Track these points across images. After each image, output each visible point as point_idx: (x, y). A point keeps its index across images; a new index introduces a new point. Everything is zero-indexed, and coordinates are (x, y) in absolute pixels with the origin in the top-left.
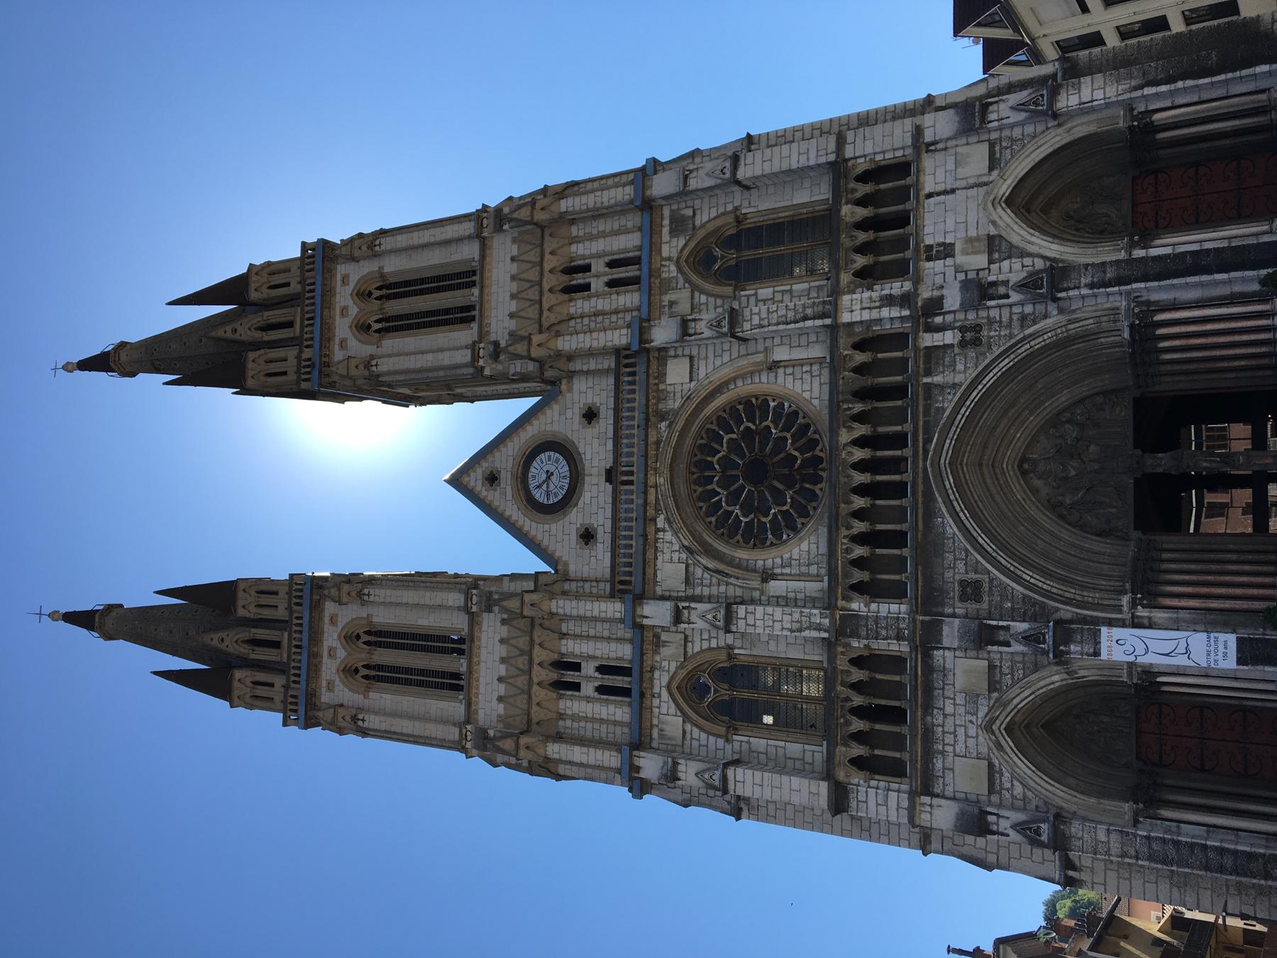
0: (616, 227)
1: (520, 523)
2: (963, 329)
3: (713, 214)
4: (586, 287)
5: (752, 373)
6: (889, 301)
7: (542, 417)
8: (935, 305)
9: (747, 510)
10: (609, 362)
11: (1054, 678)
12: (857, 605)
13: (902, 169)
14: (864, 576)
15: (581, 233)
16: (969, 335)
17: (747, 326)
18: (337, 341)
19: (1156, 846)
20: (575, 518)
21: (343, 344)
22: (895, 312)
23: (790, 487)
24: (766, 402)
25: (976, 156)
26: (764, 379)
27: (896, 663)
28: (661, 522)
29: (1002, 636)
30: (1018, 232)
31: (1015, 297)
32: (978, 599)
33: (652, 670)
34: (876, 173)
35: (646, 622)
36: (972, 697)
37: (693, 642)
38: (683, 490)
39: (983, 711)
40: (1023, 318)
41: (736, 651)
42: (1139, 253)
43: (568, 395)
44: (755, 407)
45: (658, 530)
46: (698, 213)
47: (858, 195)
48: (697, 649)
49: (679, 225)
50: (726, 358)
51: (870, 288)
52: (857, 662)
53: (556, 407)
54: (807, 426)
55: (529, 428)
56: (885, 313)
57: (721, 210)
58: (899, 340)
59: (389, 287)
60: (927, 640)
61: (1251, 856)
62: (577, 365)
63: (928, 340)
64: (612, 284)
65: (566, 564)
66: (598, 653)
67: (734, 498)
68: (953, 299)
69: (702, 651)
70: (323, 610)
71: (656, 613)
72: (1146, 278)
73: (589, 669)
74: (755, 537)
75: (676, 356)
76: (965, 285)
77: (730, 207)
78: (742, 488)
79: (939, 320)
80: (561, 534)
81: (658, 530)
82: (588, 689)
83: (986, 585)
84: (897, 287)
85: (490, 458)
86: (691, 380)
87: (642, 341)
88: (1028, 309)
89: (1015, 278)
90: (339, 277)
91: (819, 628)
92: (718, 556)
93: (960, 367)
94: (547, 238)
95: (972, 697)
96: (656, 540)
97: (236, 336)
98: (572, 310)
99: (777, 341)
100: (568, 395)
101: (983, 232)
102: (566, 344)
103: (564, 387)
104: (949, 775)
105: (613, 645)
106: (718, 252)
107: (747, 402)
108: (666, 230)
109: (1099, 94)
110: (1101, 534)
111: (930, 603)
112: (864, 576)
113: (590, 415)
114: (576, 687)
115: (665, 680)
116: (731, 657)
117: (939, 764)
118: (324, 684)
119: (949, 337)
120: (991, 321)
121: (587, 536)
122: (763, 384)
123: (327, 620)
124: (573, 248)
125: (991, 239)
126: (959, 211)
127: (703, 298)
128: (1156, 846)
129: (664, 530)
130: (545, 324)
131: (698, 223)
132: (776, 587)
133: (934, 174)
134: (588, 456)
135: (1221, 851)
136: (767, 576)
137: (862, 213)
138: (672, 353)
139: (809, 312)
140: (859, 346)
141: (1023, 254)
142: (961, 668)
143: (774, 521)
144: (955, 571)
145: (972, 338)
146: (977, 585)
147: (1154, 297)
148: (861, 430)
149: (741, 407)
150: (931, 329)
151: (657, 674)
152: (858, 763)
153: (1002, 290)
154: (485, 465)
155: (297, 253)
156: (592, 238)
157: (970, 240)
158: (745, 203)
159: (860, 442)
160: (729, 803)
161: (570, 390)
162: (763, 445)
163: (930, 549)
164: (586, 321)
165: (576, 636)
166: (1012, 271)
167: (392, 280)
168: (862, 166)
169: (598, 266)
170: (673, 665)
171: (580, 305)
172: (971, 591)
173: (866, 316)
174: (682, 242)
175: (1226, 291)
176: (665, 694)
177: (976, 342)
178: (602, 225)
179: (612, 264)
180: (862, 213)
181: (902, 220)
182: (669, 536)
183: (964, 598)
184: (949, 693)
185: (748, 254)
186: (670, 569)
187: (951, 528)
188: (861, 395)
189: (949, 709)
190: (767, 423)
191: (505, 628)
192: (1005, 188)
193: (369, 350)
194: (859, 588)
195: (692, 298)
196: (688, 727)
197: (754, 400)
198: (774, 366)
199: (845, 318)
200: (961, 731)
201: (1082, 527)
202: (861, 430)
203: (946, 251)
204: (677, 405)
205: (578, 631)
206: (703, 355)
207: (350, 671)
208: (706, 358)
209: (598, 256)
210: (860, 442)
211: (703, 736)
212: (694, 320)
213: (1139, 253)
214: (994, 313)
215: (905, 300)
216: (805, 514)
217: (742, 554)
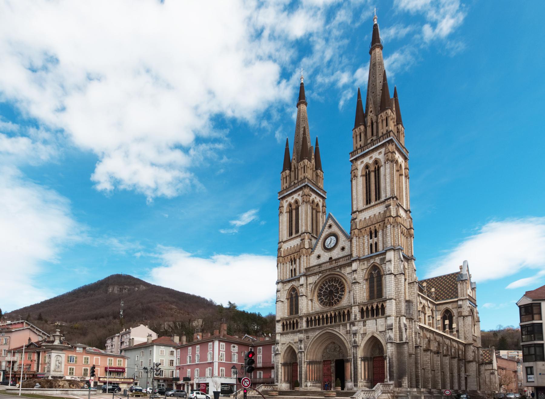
6: (356, 316)
8: (354, 325)
12: (305, 319)
14: (309, 319)
22: (353, 318)
23: (329, 300)
30: (366, 338)
31: (353, 340)
36: (293, 340)
38: (327, 277)
39: (292, 342)
44: (343, 290)
52: (297, 321)
56: (353, 316)
60: (300, 332)
63: (348, 325)
68: (354, 328)
74: (319, 295)
76: (356, 330)
89: (357, 339)
92: (315, 289)
95: (293, 340)
107: (344, 287)
111: (306, 331)
112: (309, 319)
122: (347, 290)
126: (373, 327)
132: (310, 302)
136: (311, 300)
137: (375, 307)
140: (348, 311)
145: (348, 332)
148: (333, 315)
152: (283, 323)
157: (366, 330)
159: (331, 315)
162: (335, 293)
163: (313, 330)
166: (358, 338)
169: (375, 240)
172: (308, 338)
173: (353, 312)
177: (347, 333)
180: (375, 307)
182: (318, 277)
185: (375, 280)
186: (311, 280)
187: (317, 333)
188: (339, 313)
194: (308, 319)
202: (333, 315)
203: (364, 325)
204: (343, 272)
210: (331, 315)
215: (355, 319)
217: (316, 294)
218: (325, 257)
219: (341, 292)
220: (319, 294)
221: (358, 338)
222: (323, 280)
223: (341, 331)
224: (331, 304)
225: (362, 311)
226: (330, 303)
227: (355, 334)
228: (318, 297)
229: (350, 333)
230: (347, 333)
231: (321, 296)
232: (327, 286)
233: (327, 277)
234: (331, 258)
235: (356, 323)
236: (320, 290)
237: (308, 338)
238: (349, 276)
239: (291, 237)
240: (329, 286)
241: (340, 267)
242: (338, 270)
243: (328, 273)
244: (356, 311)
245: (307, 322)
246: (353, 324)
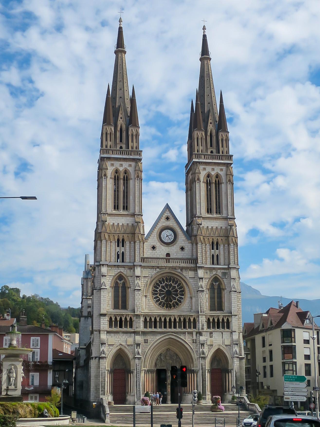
0: (226, 257)
1: (157, 228)
2: (196, 340)
3: (226, 283)
4: (213, 249)
5: (190, 292)
6: (203, 325)
7: (182, 234)
9: (160, 290)
10: (195, 257)
11: (131, 357)
12: (142, 319)
13: (228, 327)
14: (148, 320)
15: (225, 247)
16: (195, 341)
17: (200, 294)
18: (205, 167)
19: (104, 374)
20: (158, 244)
21: (205, 169)
22: (200, 327)
23: (165, 301)
24: (183, 295)
25: (227, 342)
26: (189, 295)
27: (131, 326)
28: (158, 270)
29: (138, 347)
31: (201, 350)
32: (145, 342)
33: (124, 267)
34: (228, 323)
35: (136, 268)
38: (165, 275)
39: (124, 344)
40: (197, 351)
42: (207, 372)
43: (187, 242)
44: (183, 293)
45: (156, 269)
47: (224, 319)
48: (130, 279)
49: (224, 274)
50: (194, 286)
51: (206, 321)
52: (131, 318)
53: (185, 239)
54: (178, 305)
55: (180, 230)
56: (200, 325)
58: (195, 327)
59: (218, 184)
61: (104, 388)
62: (194, 246)
63: (194, 334)
64: (213, 256)
65: (147, 241)
66: (127, 252)
67: (163, 287)
69: (129, 281)
70: (133, 162)
71: (138, 271)
72: (202, 372)
73: (123, 249)
74: (154, 293)
76: (204, 341)
78: (165, 289)
79: (198, 335)
80: (154, 240)
81: (156, 269)
82: (118, 249)
83: (147, 344)
84: (205, 326)
85: (173, 218)
87: (199, 267)
88: (199, 352)
90: (222, 168)
91: (137, 310)
92: (150, 284)
93: (189, 339)
94: (225, 238)
97: (209, 124)
98: (208, 245)
99: (197, 299)
100: (187, 242)
101: (214, 344)
102: (199, 245)
103: (190, 241)
104: (111, 337)
105: (129, 257)
106: (217, 284)
107: (183, 291)
108: (223, 271)
109: (236, 365)
110: (156, 363)
111: (144, 333)
112: (148, 320)
113: (182, 249)
114: (118, 246)
115: (122, 271)
116: (128, 288)
117: (113, 335)
118: (113, 162)
119: (195, 337)
120: (197, 345)
121: (154, 248)
122: (188, 295)
123: (130, 163)
124: (222, 245)
125: (212, 345)
127: (207, 281)
128: (104, 374)
130: (205, 237)
131: (224, 279)
133: (226, 335)
134: (173, 248)
135: (105, 384)
139: (202, 308)
141: (209, 351)
142: (130, 340)
143: (158, 297)
144: (150, 338)
146: (147, 342)
147: (199, 373)
150: (197, 333)
151: (123, 269)
152: (111, 318)
153: (202, 348)
154: (171, 216)
155: (230, 154)
156: (224, 250)
157: (213, 341)
161: (189, 243)
162: (174, 294)
164: (205, 249)
165: (130, 246)
166: (206, 349)
167: (220, 186)
168: (230, 319)
170: (125, 273)
171: (208, 247)
172: (146, 341)
174: (220, 275)
175: (199, 385)
176: (119, 271)
177: (193, 342)
178: (227, 253)
179: (217, 256)
181: (218, 327)
182: (155, 272)
183: (145, 340)
184: (127, 337)
187: (158, 338)
188: (185, 320)
189: (123, 337)
190: (179, 296)
191: (131, 225)
192: (221, 348)
193: (202, 179)
194: (146, 319)
196: (112, 277)
198: (191, 298)
199: (200, 316)
200: (119, 339)
201: (157, 359)
203: (211, 337)
204: (184, 274)
205: (132, 247)
207: (117, 171)
209: (219, 252)
211: (110, 281)
213: (207, 372)
214: (198, 346)
215: (203, 329)
216: (160, 304)
217: (151, 290)
218: (162, 251)
219: (180, 295)
220: (154, 290)
221: (206, 349)
222: (160, 276)
223: (187, 339)
224: (169, 306)
225: (208, 321)
226: (167, 305)
227: (203, 345)
228: (154, 294)
229: (196, 343)
230: (193, 342)
231: (157, 294)
232: (164, 285)
233: (165, 275)
234: (168, 255)
235: (203, 333)
236: (155, 287)
237: (146, 341)
238: (191, 280)
239: (115, 212)
240: (166, 285)
241: (182, 269)
242: (179, 270)
243: (167, 270)
244: (202, 320)
245: (145, 321)
246: (200, 334)
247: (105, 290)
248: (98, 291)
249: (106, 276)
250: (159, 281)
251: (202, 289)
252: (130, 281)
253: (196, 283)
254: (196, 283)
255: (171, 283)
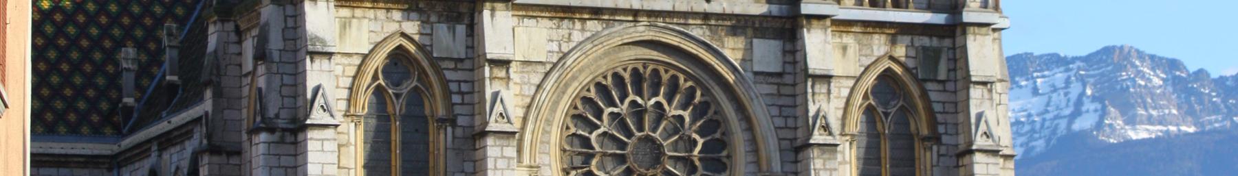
3: (937, 107)
28: (593, 26)
37: (456, 69)
41: (449, 129)
46: (940, 87)
57: (940, 117)
75: (785, 52)
77: (941, 129)
86: (756, 73)
96: (571, 19)
108: (926, 41)
129: (583, 30)
138: (789, 47)
149: (717, 135)
158: (943, 150)
160: (277, 116)
176: (393, 27)
182: (577, 37)
195: (847, 77)
196: (357, 61)
197: (724, 153)
206: (785, 90)
208: (780, 95)
212: (829, 92)
243: (642, 31)
247: (329, 133)
248: (282, 141)
249: (329, 55)
250: (598, 85)
251: (829, 140)
252: (453, 87)
253: (788, 101)
254: (788, 101)
255: (661, 99)
